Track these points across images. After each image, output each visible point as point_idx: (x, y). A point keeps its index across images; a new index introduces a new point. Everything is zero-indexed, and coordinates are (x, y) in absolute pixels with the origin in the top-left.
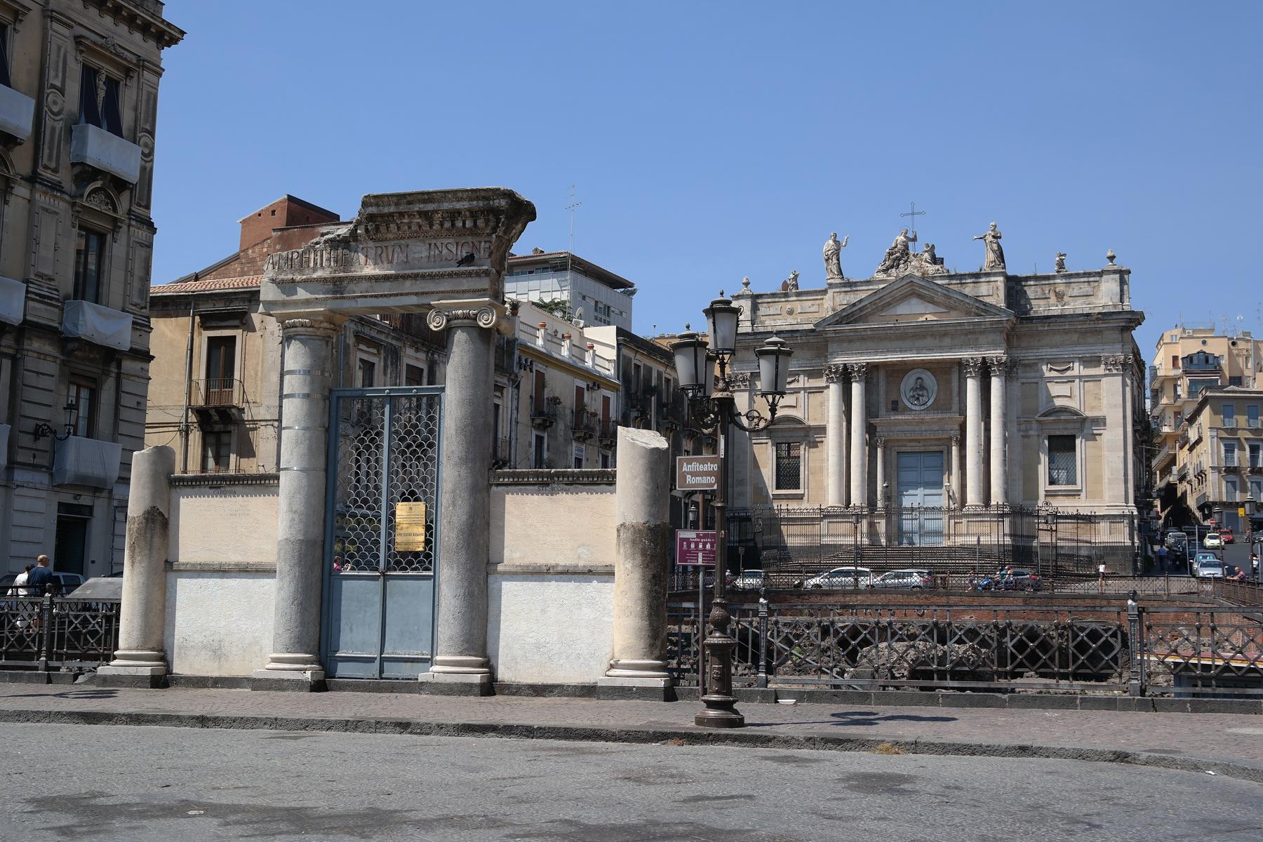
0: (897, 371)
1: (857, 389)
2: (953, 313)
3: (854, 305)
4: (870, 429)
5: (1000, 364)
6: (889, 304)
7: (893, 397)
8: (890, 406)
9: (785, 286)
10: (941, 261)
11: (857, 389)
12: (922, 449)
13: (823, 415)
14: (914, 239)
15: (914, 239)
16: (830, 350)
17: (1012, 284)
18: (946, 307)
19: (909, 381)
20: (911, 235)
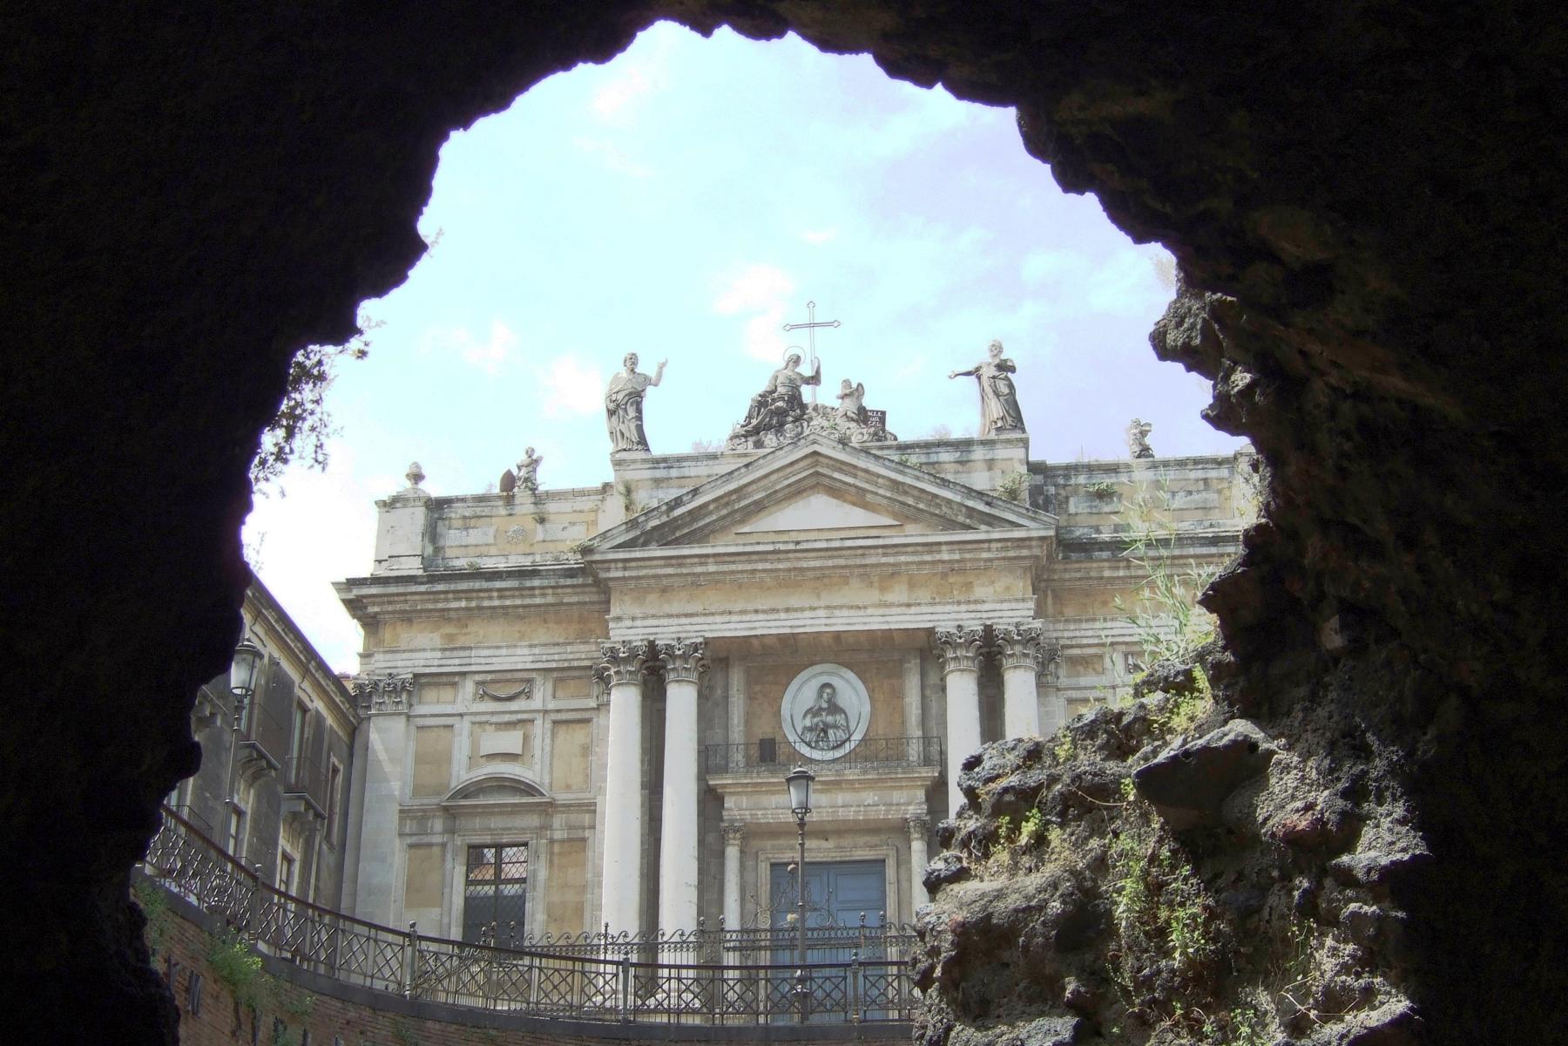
0: (774, 660)
1: (681, 700)
2: (910, 528)
3: (678, 502)
4: (710, 801)
5: (1030, 639)
6: (759, 507)
7: (763, 729)
8: (755, 752)
9: (509, 481)
10: (882, 416)
11: (681, 700)
12: (837, 856)
13: (587, 776)
14: (815, 379)
15: (815, 379)
16: (615, 610)
17: (1039, 479)
18: (895, 515)
19: (800, 697)
20: (806, 370)
